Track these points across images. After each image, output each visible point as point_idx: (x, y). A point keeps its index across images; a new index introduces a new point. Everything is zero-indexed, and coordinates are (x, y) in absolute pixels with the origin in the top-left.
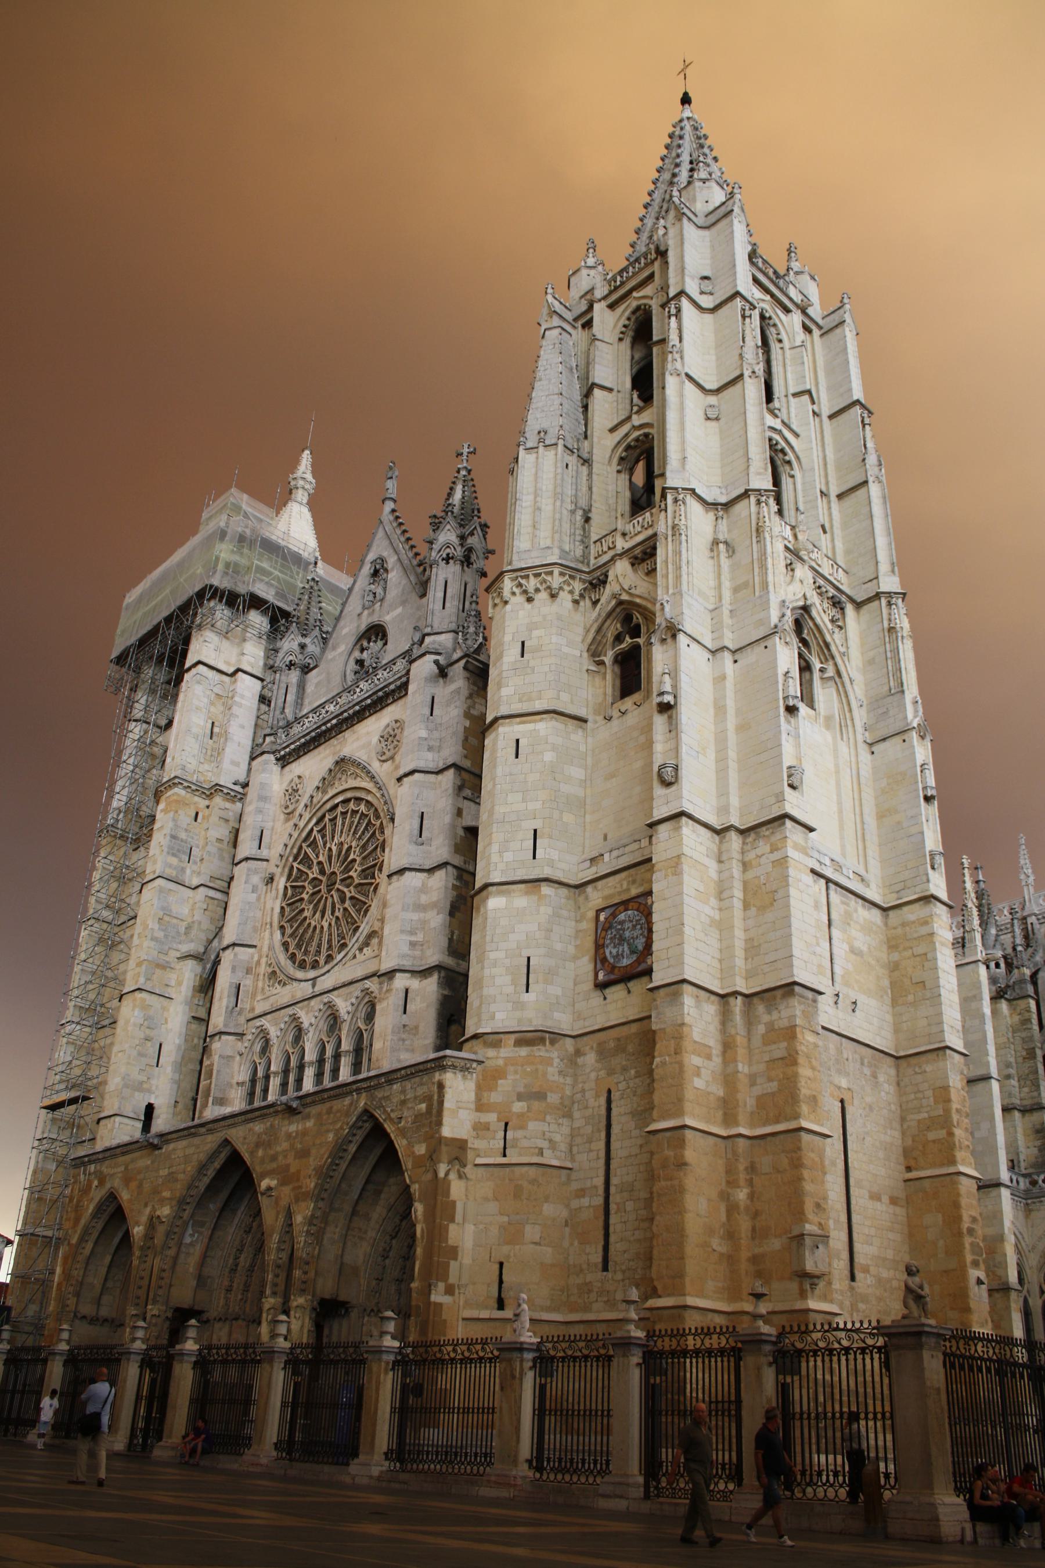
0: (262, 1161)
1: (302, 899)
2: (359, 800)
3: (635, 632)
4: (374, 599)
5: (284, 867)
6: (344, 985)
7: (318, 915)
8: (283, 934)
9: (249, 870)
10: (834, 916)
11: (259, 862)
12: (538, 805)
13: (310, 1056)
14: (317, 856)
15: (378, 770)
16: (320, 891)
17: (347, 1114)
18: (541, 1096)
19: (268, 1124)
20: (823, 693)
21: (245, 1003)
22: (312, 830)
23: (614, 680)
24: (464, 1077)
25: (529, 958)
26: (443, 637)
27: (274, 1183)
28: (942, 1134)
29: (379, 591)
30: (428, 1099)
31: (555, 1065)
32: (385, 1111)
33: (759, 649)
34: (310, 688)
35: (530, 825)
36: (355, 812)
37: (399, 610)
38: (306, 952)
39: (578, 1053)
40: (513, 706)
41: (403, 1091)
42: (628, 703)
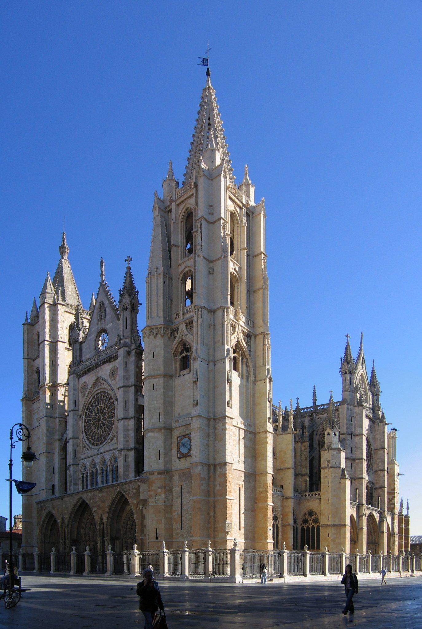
1: (91, 423)
2: (105, 392)
5: (84, 413)
6: (107, 451)
7: (96, 429)
8: (86, 434)
9: (73, 414)
11: (76, 411)
13: (99, 471)
14: (94, 410)
15: (110, 383)
22: (91, 401)
23: (181, 363)
24: (145, 484)
27: (96, 509)
30: (135, 489)
32: (125, 492)
35: (158, 411)
41: (129, 487)
42: (185, 372)
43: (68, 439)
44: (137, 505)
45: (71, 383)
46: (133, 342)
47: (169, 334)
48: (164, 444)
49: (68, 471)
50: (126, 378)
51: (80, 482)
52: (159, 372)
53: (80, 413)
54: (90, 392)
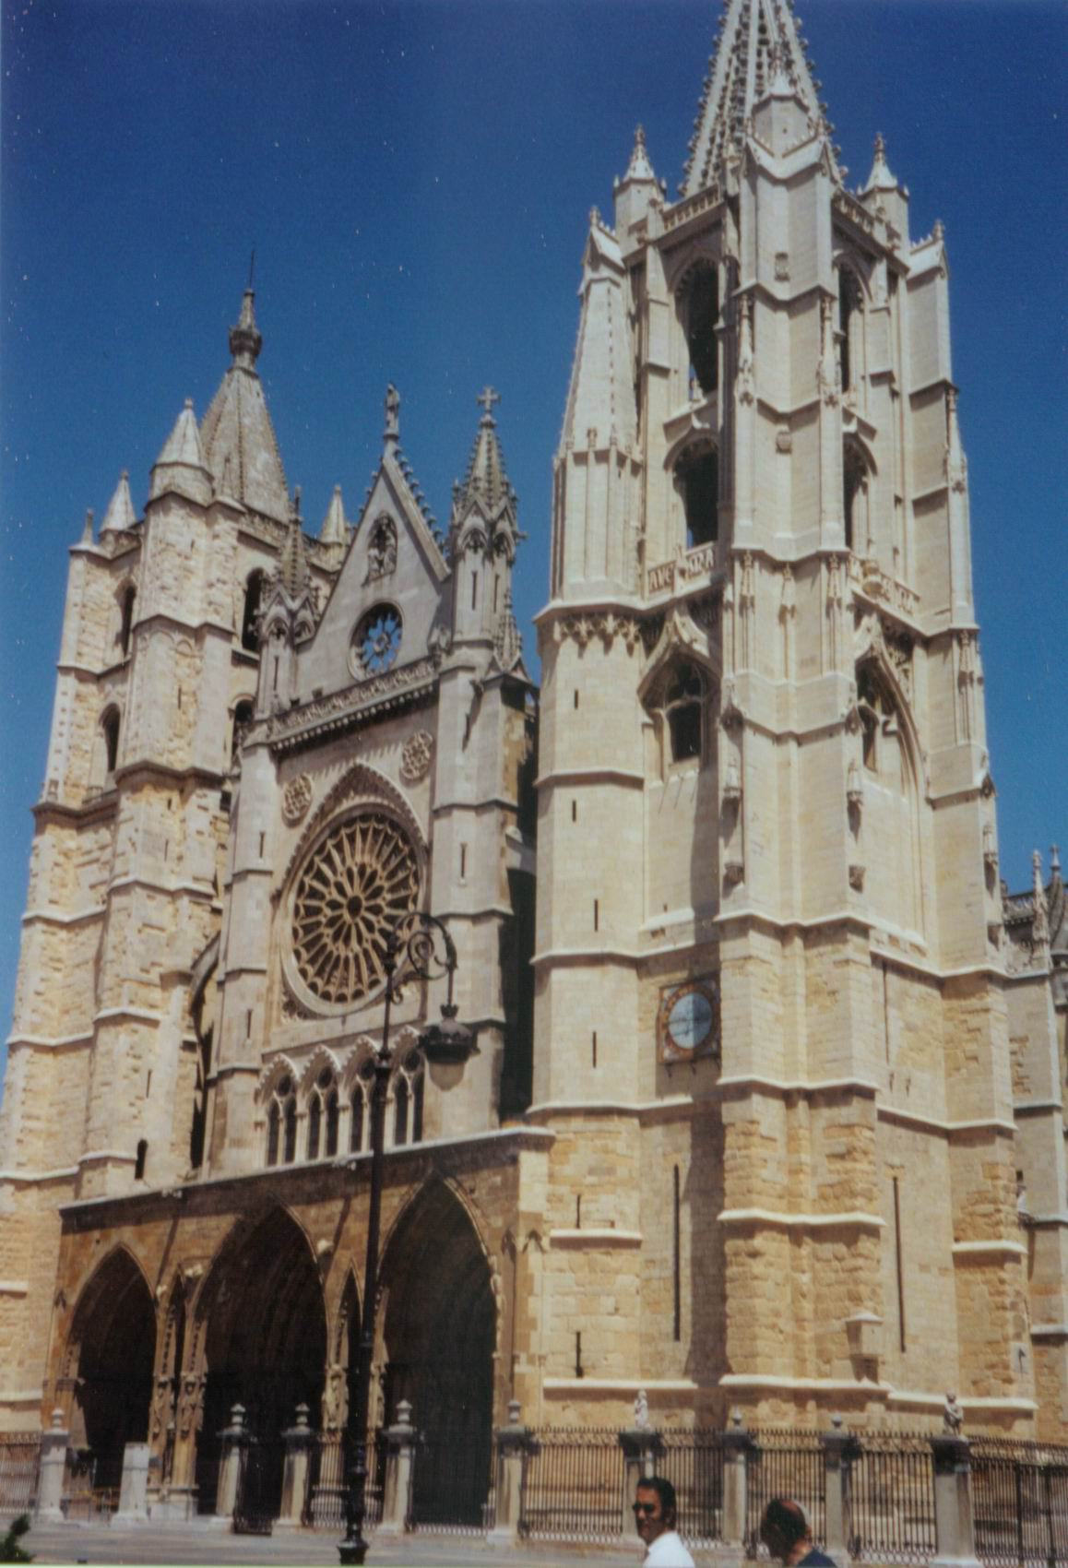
0: (316, 1222)
3: (695, 690)
4: (381, 570)
10: (891, 994)
16: (340, 916)
18: (610, 1171)
19: (321, 1184)
20: (887, 750)
21: (258, 1033)
25: (595, 1035)
28: (989, 1208)
29: (386, 557)
31: (624, 1135)
36: (376, 832)
37: (414, 592)
38: (328, 982)
47: (631, 637)
54: (323, 812)
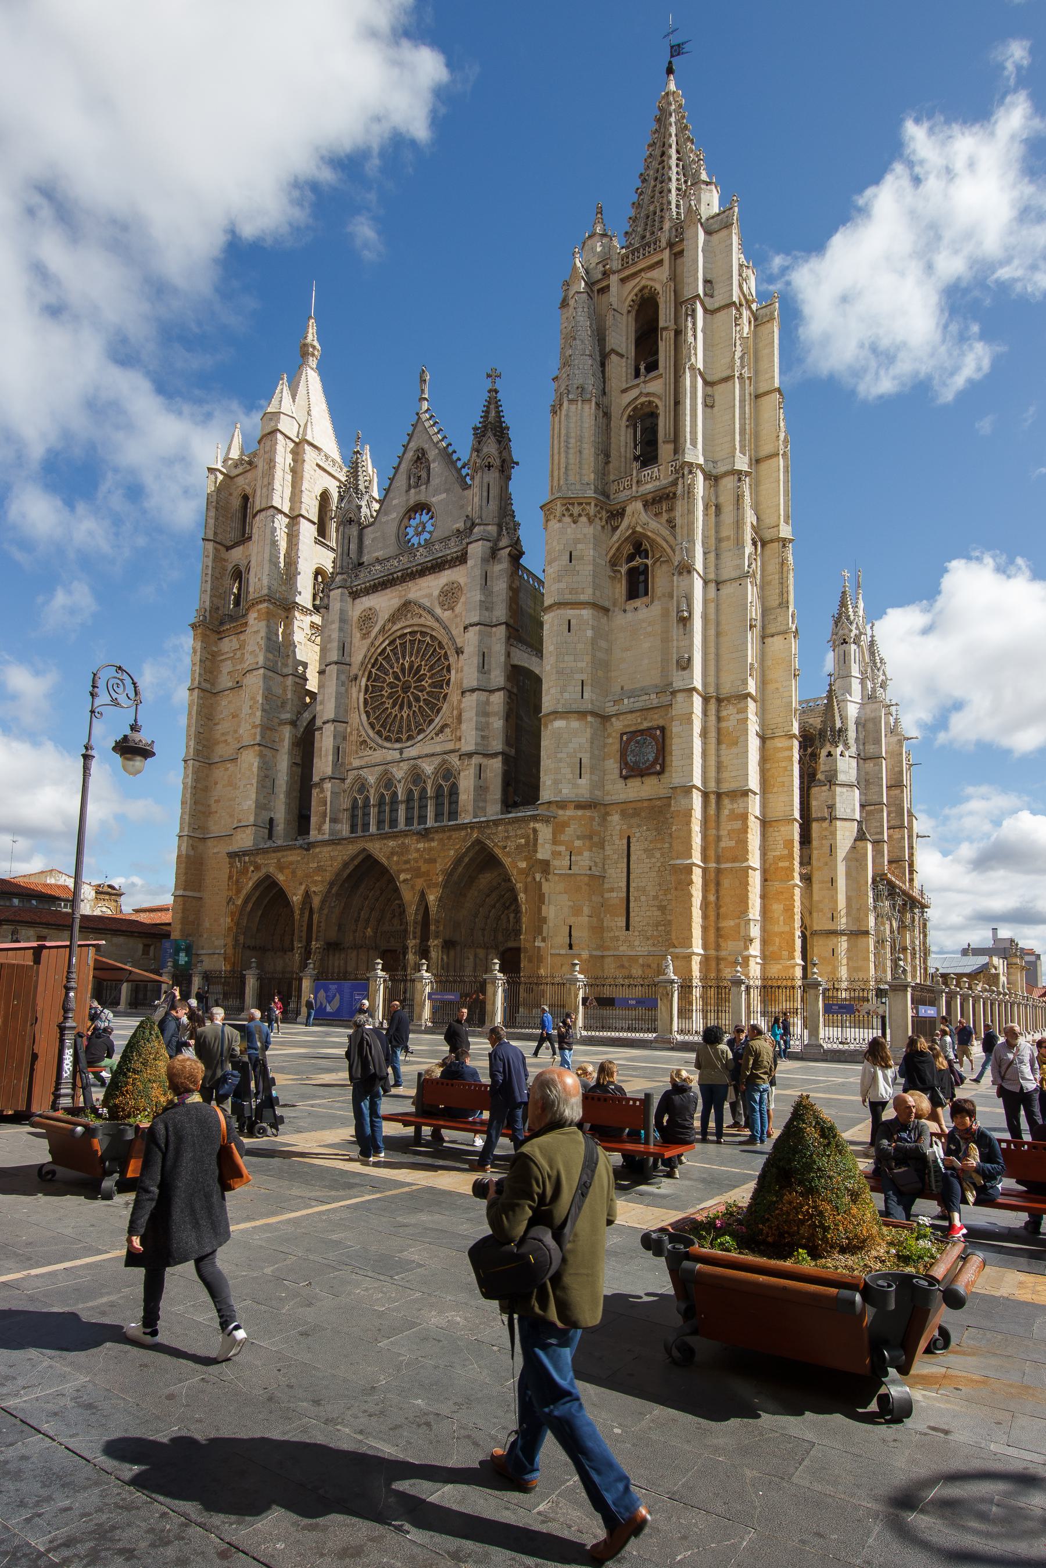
1: (382, 695)
6: (427, 756)
8: (368, 717)
12: (584, 665)
13: (401, 795)
17: (464, 841)
18: (591, 838)
22: (385, 648)
26: (490, 528)
29: (424, 474)
33: (736, 584)
34: (367, 542)
35: (579, 677)
37: (444, 496)
39: (607, 814)
40: (566, 597)
43: (319, 723)
44: (527, 873)
45: (335, 606)
46: (504, 532)
48: (591, 747)
49: (315, 792)
50: (486, 606)
51: (345, 816)
52: (583, 598)
53: (354, 670)
54: (383, 629)
